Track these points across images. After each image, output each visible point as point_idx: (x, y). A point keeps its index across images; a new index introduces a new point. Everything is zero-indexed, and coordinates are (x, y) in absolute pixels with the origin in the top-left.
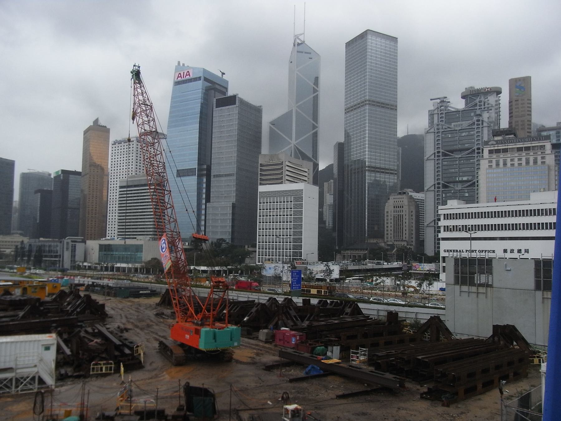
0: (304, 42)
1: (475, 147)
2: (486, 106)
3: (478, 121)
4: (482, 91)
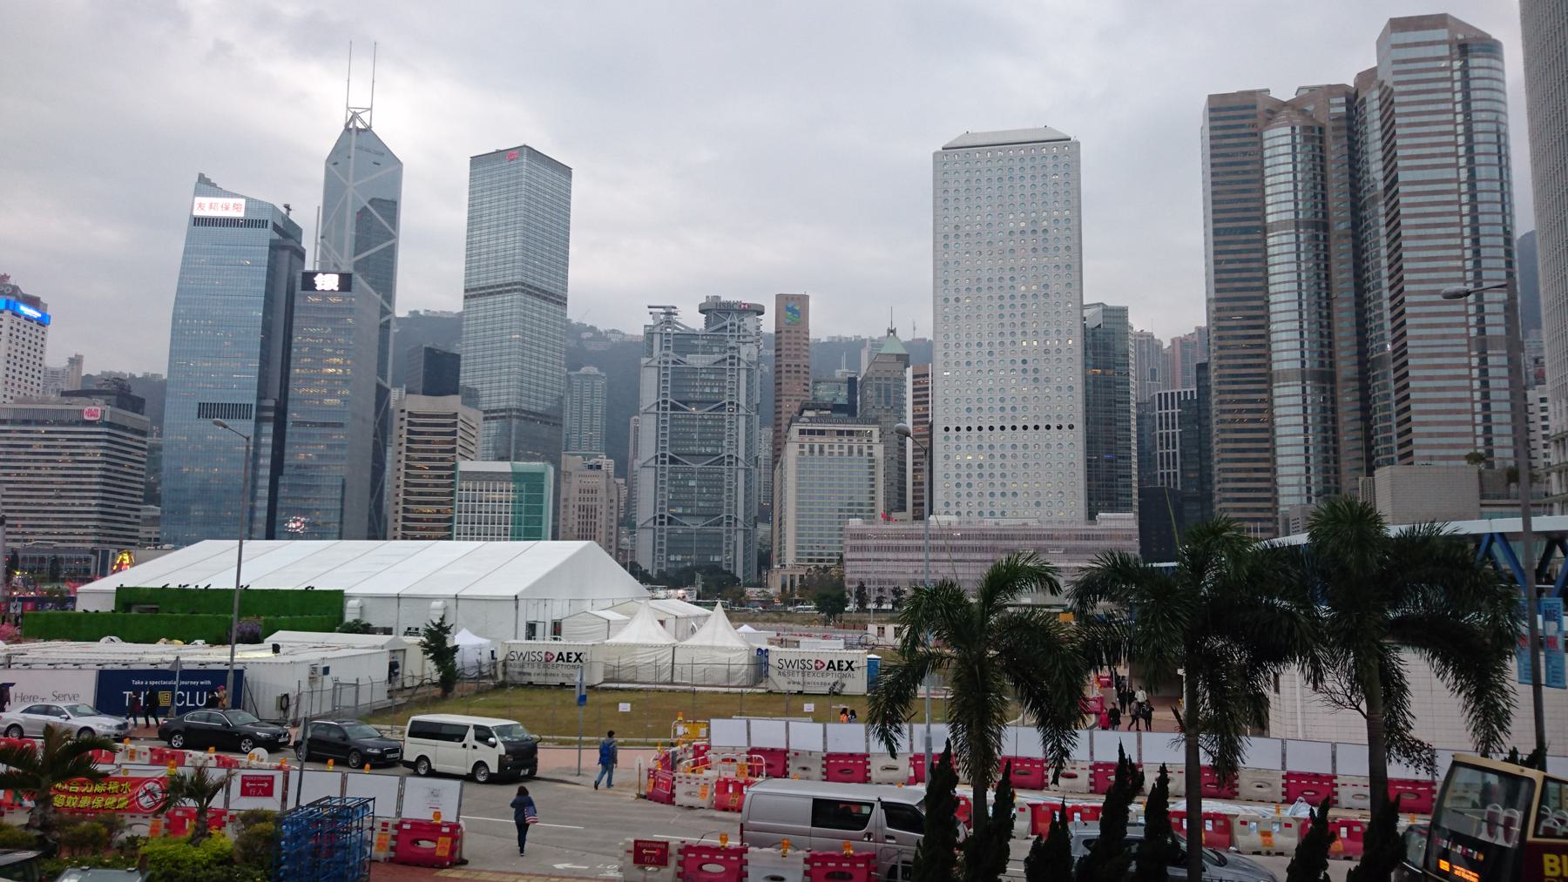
0: (370, 127)
1: (726, 401)
2: (742, 333)
3: (732, 357)
4: (736, 307)
